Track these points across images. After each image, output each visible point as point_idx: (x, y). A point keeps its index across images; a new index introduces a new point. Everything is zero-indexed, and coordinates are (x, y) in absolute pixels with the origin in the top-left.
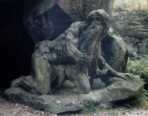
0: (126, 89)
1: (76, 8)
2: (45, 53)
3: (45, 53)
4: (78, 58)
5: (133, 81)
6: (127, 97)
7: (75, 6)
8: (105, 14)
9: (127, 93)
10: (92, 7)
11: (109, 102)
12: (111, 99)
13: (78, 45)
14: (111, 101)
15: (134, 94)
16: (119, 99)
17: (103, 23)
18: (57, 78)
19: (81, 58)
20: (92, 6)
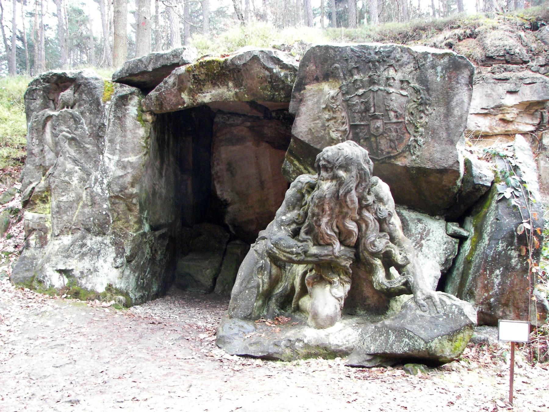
0: (406, 331)
1: (339, 135)
2: (264, 238)
3: (264, 238)
4: (285, 254)
5: (438, 313)
6: (406, 349)
7: (337, 130)
8: (340, 154)
9: (407, 340)
10: (372, 128)
11: (368, 354)
12: (372, 348)
13: (294, 226)
14: (372, 352)
15: (422, 346)
16: (387, 351)
17: (334, 175)
18: (293, 288)
19: (292, 253)
20: (372, 126)
